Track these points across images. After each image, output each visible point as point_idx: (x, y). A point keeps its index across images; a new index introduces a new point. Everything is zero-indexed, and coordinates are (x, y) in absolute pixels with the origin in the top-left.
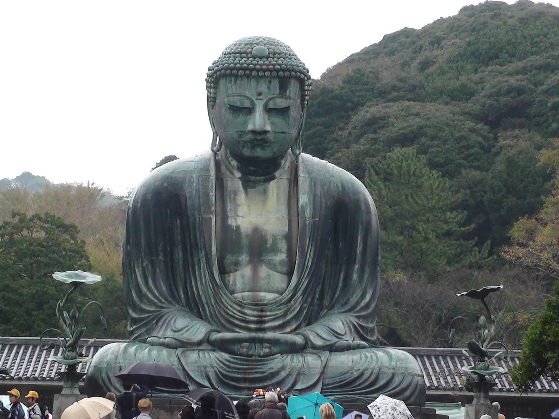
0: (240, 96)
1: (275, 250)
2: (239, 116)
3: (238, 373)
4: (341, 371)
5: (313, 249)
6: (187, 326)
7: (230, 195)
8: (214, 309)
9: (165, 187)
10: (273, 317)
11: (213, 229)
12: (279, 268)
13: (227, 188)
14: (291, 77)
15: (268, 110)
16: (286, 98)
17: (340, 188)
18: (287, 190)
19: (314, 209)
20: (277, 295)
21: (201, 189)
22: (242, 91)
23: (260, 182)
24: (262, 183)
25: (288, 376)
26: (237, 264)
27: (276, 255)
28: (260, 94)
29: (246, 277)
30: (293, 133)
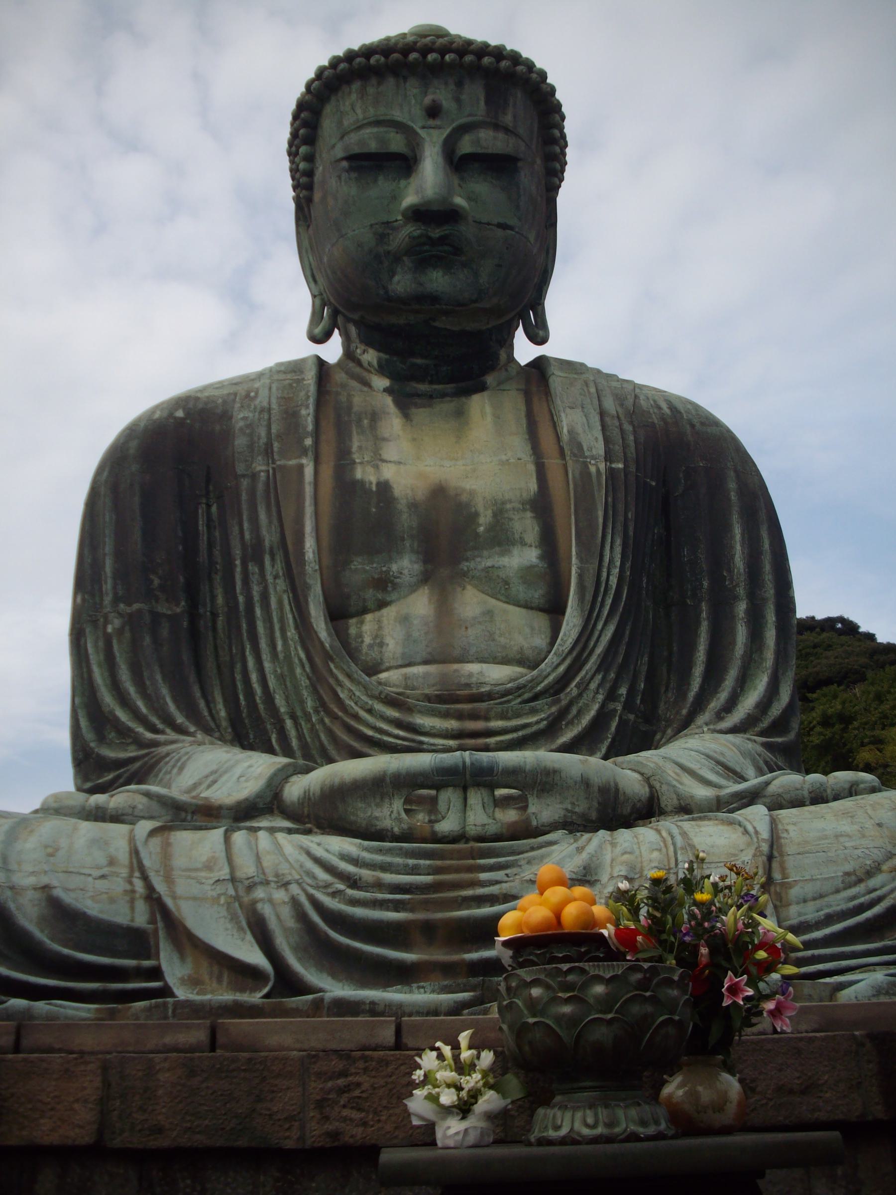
0: (378, 123)
1: (501, 538)
2: (376, 181)
3: (397, 906)
4: (848, 868)
5: (618, 541)
6: (214, 772)
7: (359, 420)
8: (313, 729)
9: (175, 418)
10: (515, 735)
11: (308, 490)
12: (519, 590)
13: (350, 407)
15: (458, 163)
16: (507, 130)
17: (668, 411)
18: (523, 408)
19: (607, 441)
20: (519, 670)
21: (274, 406)
23: (443, 395)
24: (448, 399)
27: (505, 552)
28: (433, 112)
29: (415, 622)
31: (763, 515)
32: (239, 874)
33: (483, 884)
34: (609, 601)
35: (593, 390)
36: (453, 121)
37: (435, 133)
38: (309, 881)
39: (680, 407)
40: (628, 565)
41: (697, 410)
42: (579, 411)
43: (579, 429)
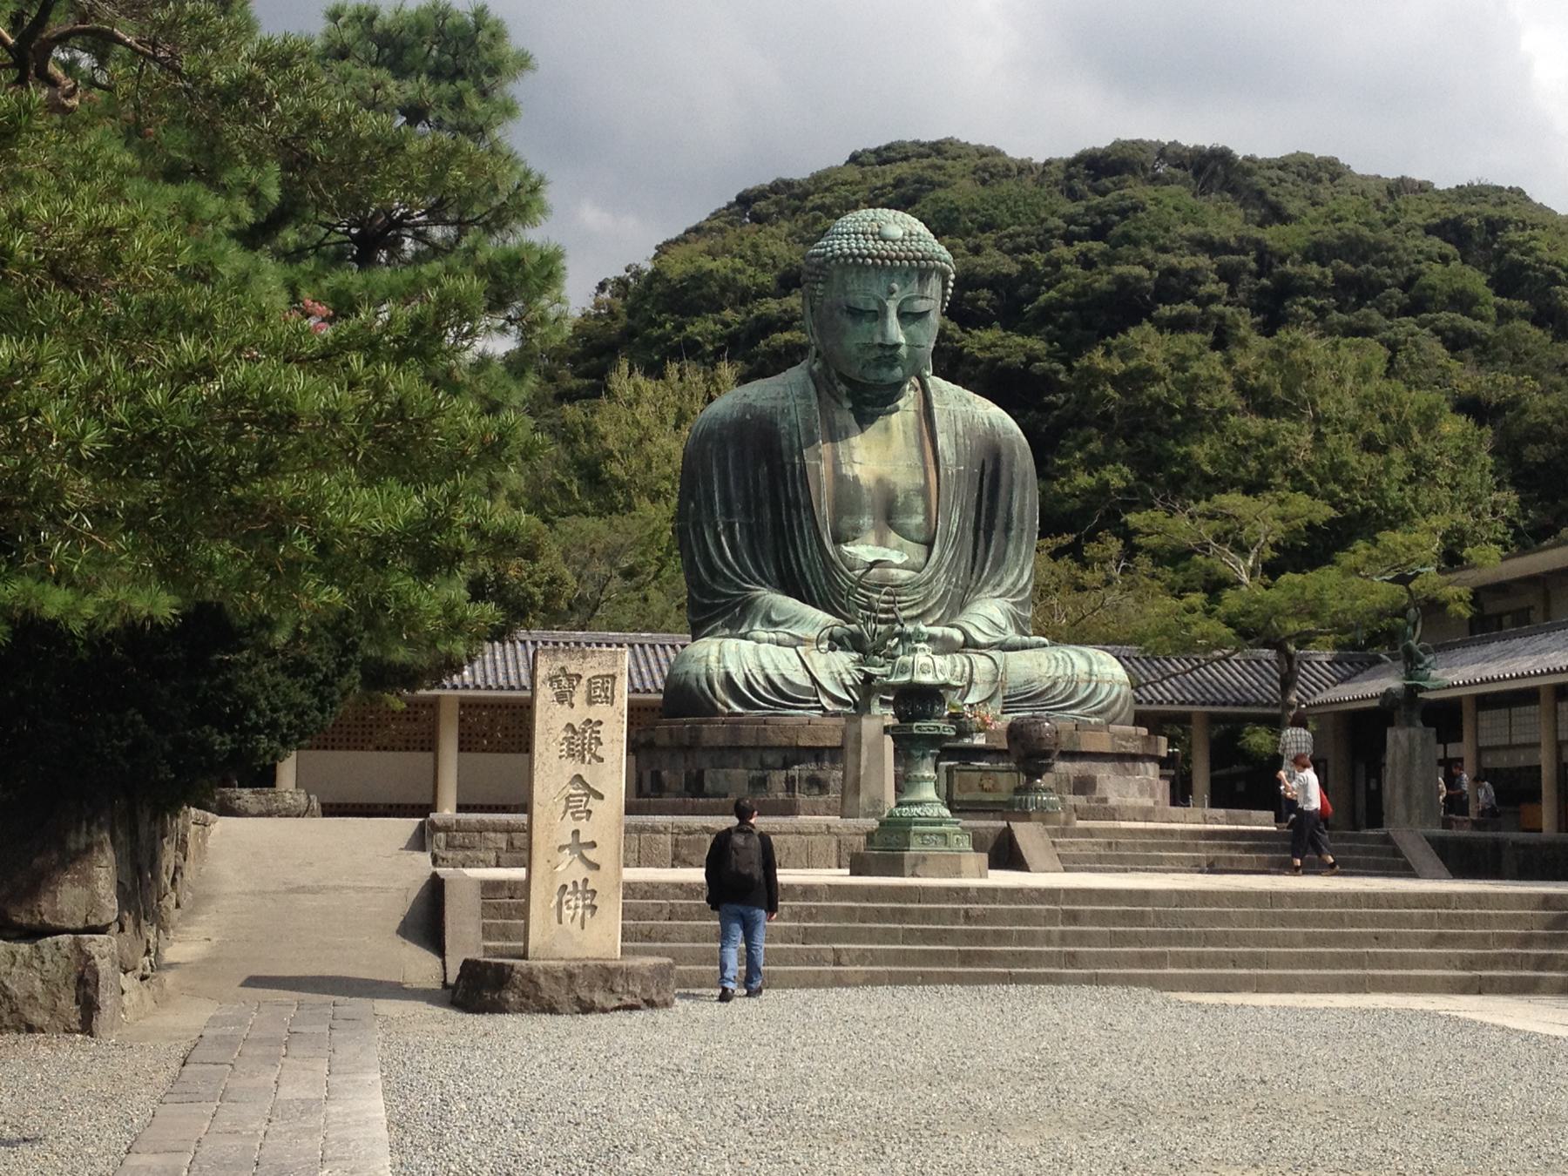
1: (908, 511)
11: (824, 479)
14: (936, 267)
28: (892, 292)
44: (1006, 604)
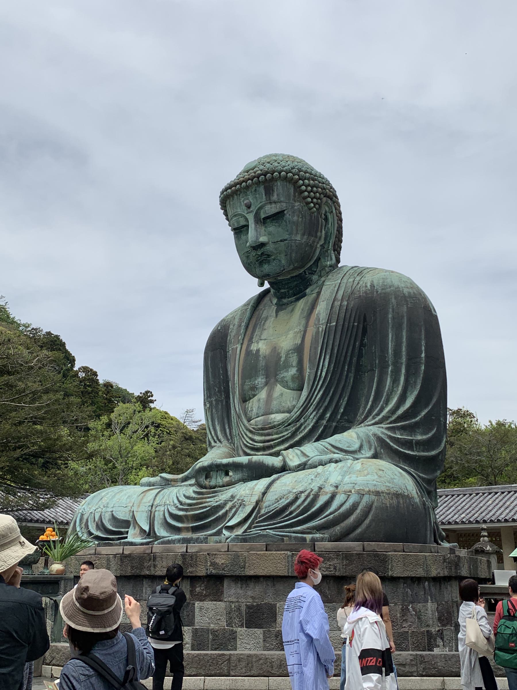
0: (235, 216)
1: (287, 366)
3: (186, 510)
4: (277, 497)
5: (328, 357)
10: (280, 440)
12: (290, 384)
14: (273, 179)
15: (263, 221)
16: (275, 202)
17: (369, 287)
20: (287, 415)
22: (235, 210)
23: (292, 302)
25: (231, 509)
26: (254, 388)
27: (287, 371)
28: (249, 207)
30: (298, 238)
31: (405, 325)
32: (155, 503)
33: (207, 502)
34: (321, 383)
35: (336, 289)
36: (256, 207)
37: (251, 214)
38: (172, 504)
39: (375, 284)
40: (332, 365)
41: (384, 282)
42: (325, 302)
43: (322, 311)
44: (380, 430)
